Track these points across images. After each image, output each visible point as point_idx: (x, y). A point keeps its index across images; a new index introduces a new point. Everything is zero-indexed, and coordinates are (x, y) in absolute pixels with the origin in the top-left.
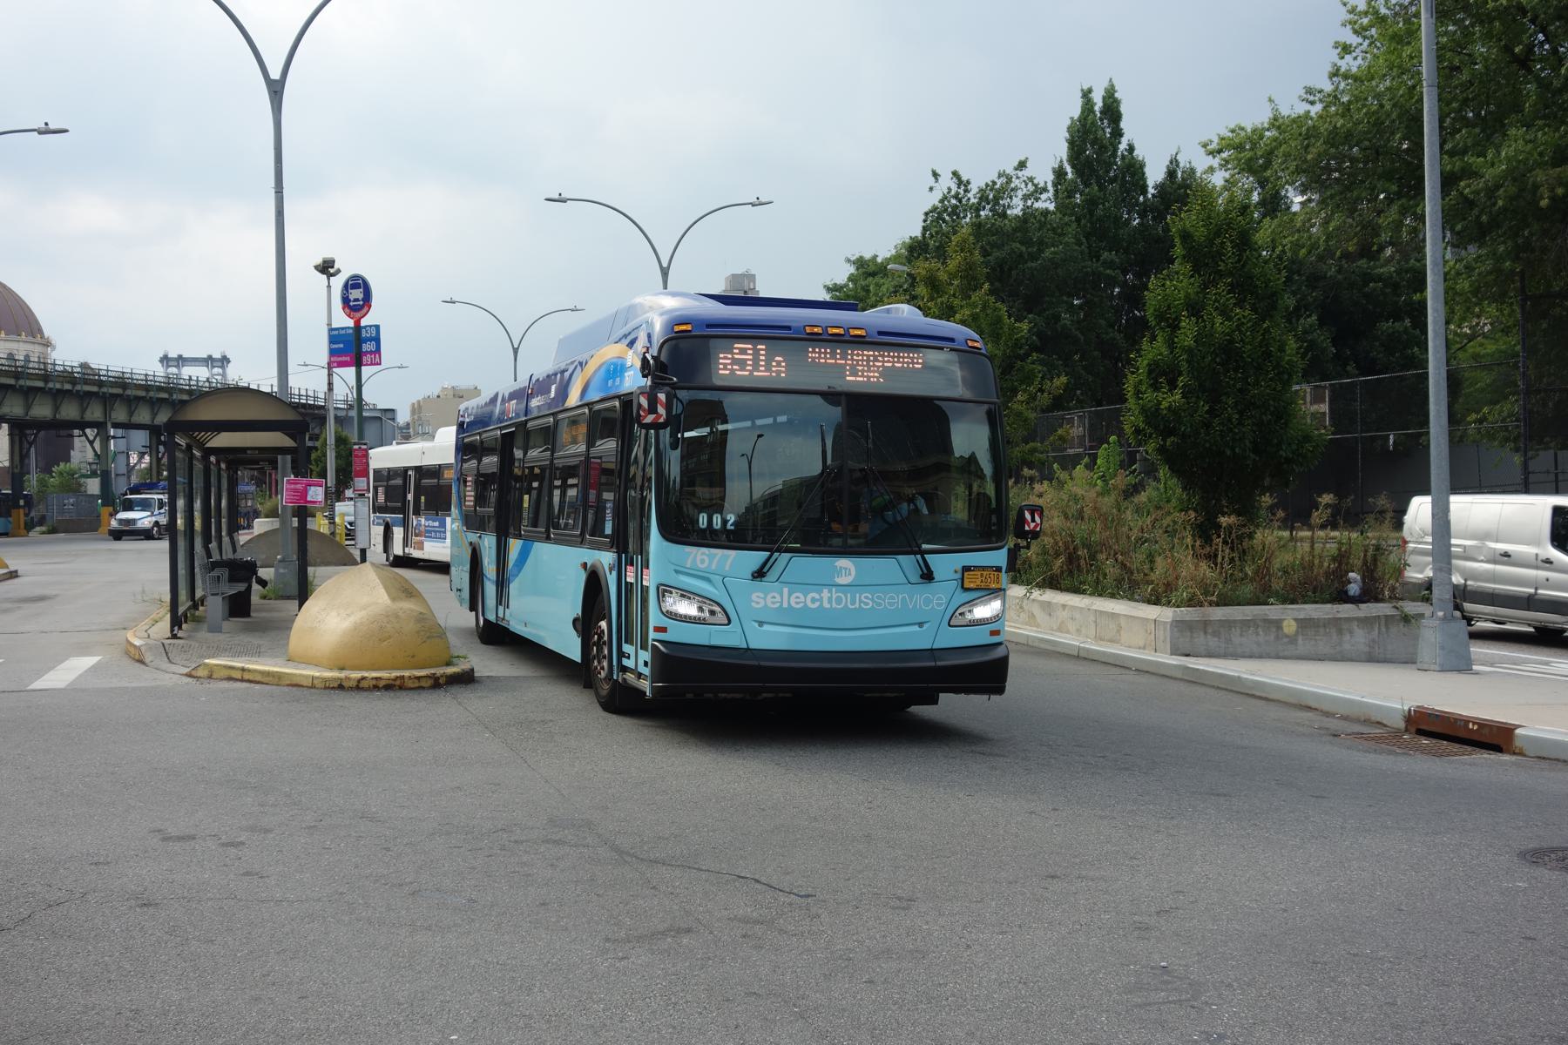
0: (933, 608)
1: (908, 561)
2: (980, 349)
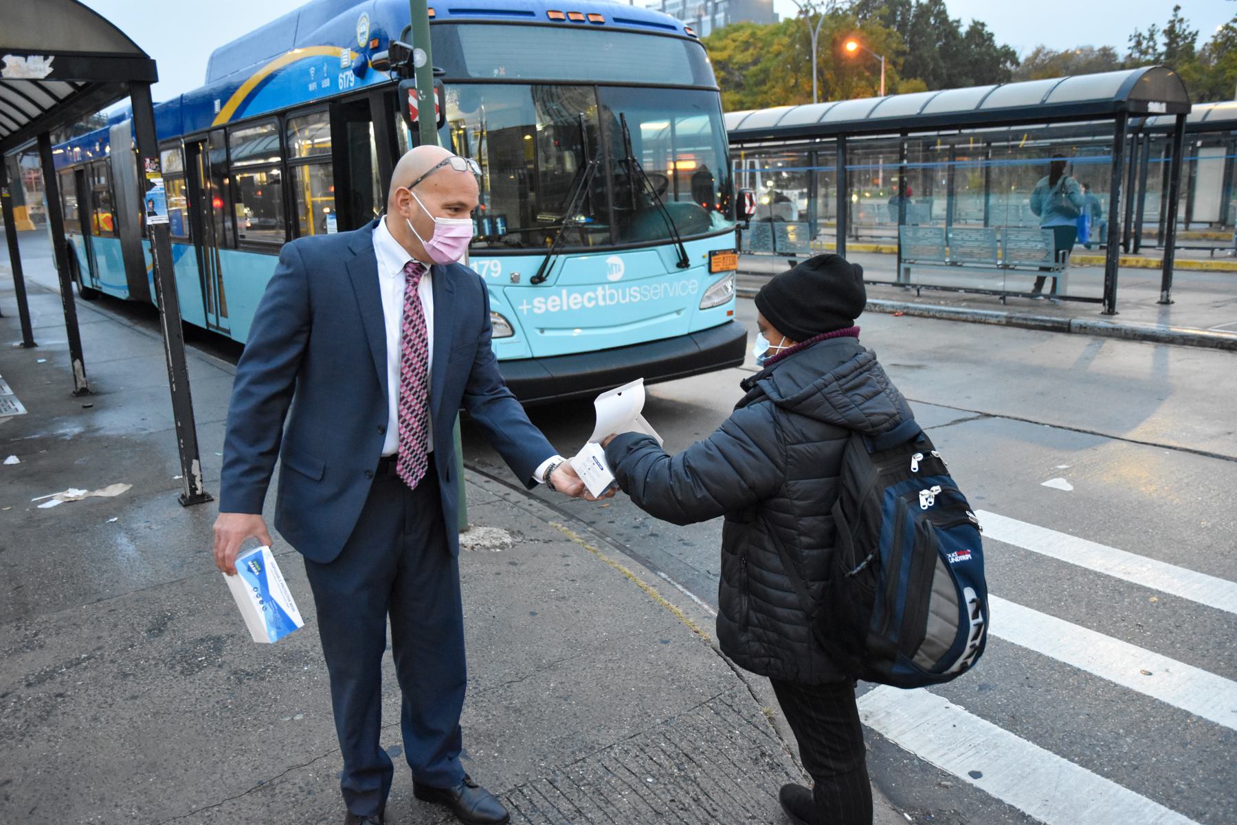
0: (689, 293)
1: (668, 252)
2: (695, 37)
